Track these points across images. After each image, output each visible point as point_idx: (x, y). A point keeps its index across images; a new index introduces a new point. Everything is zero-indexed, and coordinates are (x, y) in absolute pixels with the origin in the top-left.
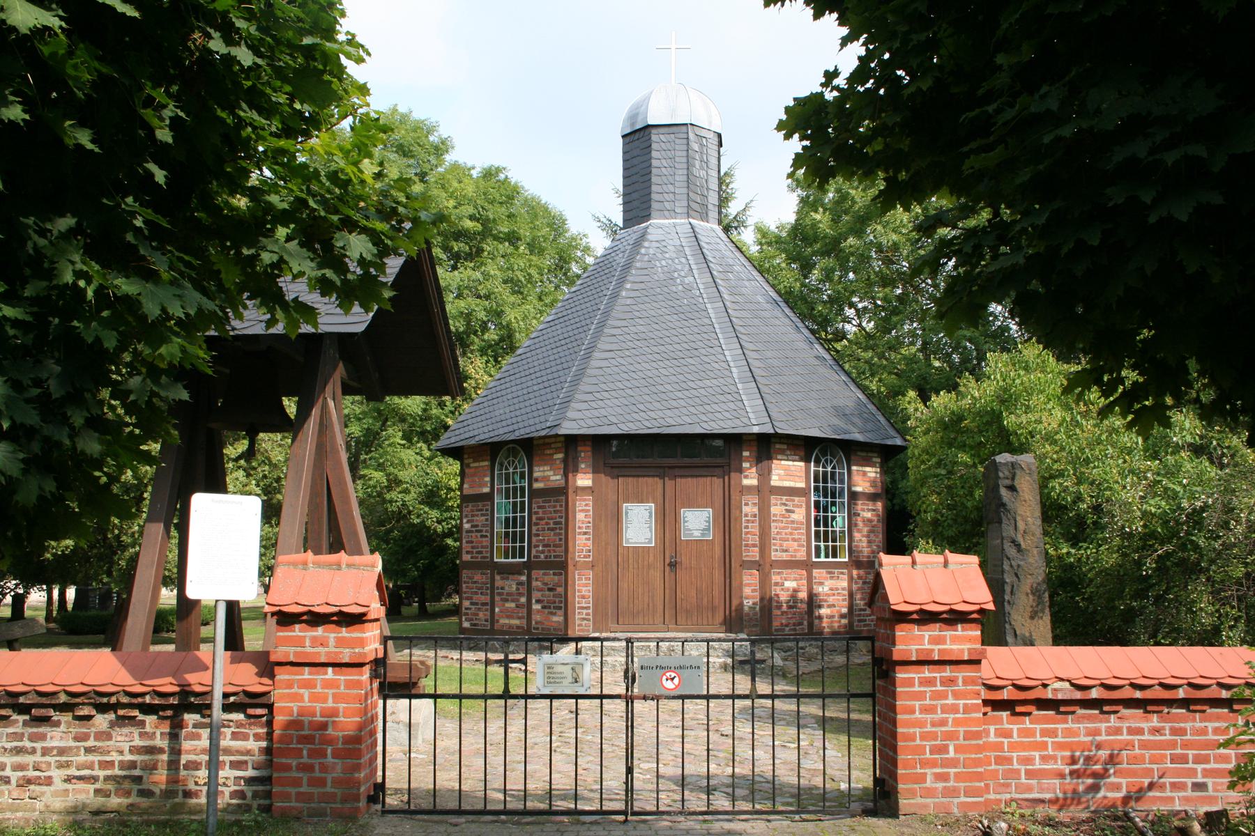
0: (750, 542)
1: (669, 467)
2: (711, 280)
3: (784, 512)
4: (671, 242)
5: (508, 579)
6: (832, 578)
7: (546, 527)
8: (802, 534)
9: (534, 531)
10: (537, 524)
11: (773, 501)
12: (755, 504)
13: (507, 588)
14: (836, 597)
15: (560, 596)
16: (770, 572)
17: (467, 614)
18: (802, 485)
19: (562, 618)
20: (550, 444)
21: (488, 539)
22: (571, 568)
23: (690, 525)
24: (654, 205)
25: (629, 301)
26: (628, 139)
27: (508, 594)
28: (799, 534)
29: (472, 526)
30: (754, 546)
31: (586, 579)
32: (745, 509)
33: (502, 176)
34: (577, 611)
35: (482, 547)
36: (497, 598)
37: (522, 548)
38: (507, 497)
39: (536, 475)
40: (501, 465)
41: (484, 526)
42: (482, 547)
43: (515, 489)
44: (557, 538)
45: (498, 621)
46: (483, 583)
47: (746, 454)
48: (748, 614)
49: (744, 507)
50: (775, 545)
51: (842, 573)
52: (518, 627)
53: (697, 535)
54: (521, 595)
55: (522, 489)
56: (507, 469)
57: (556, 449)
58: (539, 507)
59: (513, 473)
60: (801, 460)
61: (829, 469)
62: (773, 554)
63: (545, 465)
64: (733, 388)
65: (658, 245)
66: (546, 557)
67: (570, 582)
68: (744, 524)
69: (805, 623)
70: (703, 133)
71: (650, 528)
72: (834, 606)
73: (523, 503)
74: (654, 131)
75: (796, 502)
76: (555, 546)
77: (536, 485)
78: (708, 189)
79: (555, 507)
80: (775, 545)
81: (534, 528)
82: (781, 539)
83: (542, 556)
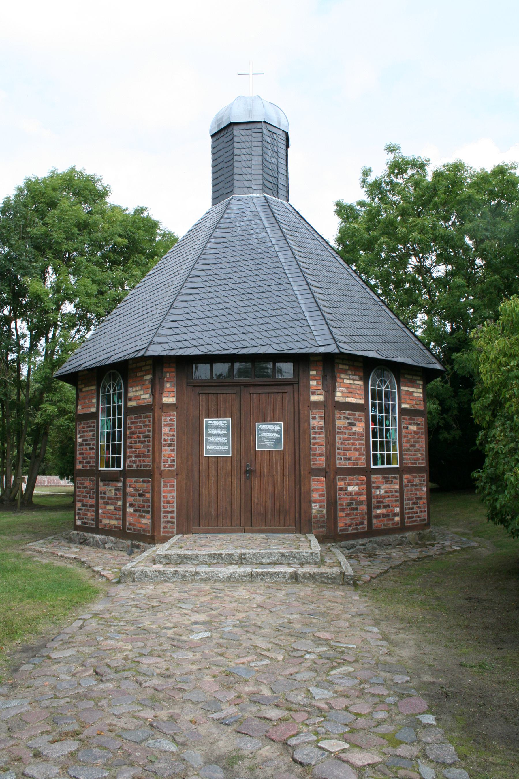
0: (317, 452)
1: (246, 386)
2: (281, 235)
3: (347, 425)
4: (249, 209)
5: (108, 485)
6: (387, 482)
7: (138, 440)
8: (362, 444)
9: (128, 444)
10: (130, 438)
11: (337, 415)
12: (321, 418)
13: (107, 493)
14: (390, 499)
15: (147, 501)
16: (335, 479)
17: (79, 514)
18: (361, 401)
19: (150, 521)
20: (141, 367)
21: (94, 451)
22: (157, 476)
23: (263, 437)
24: (236, 184)
25: (212, 251)
26: (215, 139)
27: (110, 498)
28: (359, 444)
29: (84, 441)
30: (321, 455)
31: (171, 486)
32: (314, 422)
33: (145, 214)
34: (162, 515)
35: (91, 458)
36: (101, 501)
37: (119, 458)
38: (109, 416)
39: (130, 395)
40: (104, 388)
41: (92, 440)
42: (91, 458)
43: (114, 407)
44: (146, 450)
45: (101, 522)
46: (90, 488)
47: (313, 373)
48: (316, 517)
49: (311, 420)
50: (339, 454)
51: (395, 478)
52: (116, 527)
53: (270, 446)
54: (118, 499)
55: (120, 407)
56: (108, 391)
57: (146, 371)
58: (132, 423)
59: (113, 394)
60: (360, 379)
61: (383, 388)
62: (338, 462)
63: (138, 385)
64: (301, 316)
65: (238, 211)
66: (137, 466)
67: (156, 489)
68: (312, 436)
69: (366, 522)
70: (274, 130)
71: (228, 439)
72: (389, 506)
73: (120, 419)
74: (235, 128)
75: (357, 417)
76: (144, 457)
77: (131, 404)
78: (278, 172)
79: (144, 422)
80: (339, 454)
81: (128, 441)
82: (345, 449)
83: (134, 465)
